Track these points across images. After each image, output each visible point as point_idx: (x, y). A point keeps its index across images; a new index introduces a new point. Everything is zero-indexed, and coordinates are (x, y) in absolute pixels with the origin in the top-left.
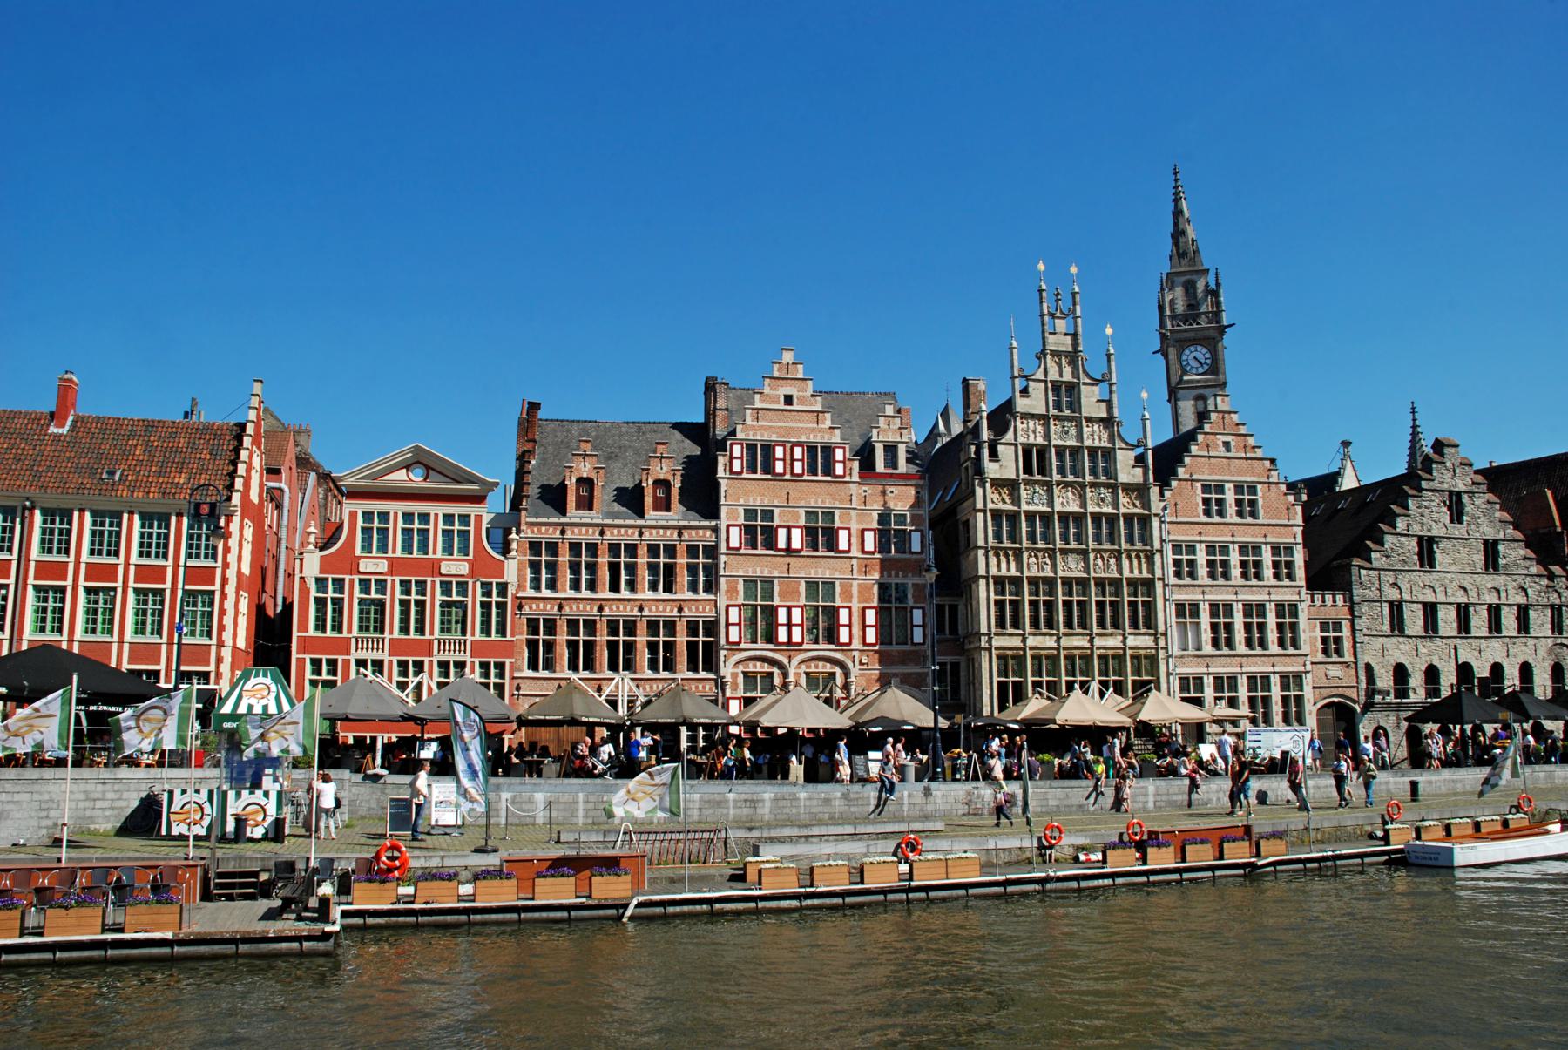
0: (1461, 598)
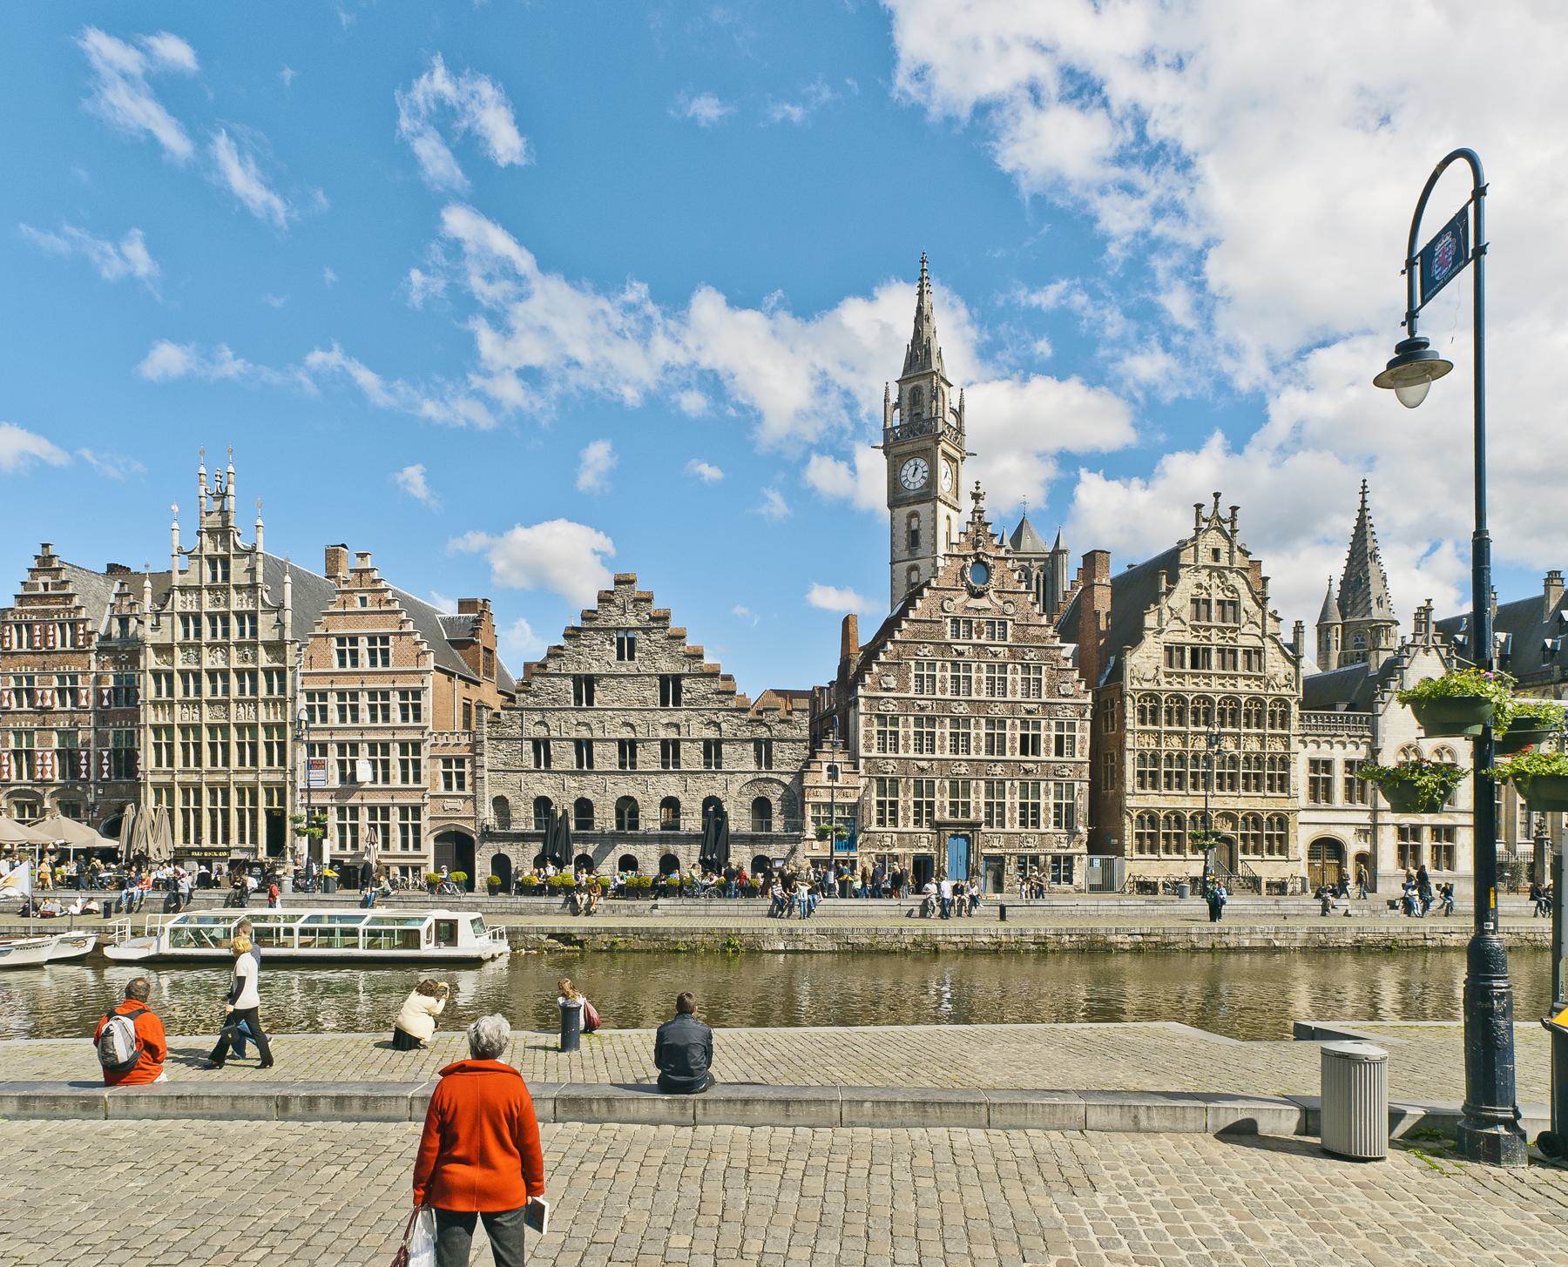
0: (626, 734)
